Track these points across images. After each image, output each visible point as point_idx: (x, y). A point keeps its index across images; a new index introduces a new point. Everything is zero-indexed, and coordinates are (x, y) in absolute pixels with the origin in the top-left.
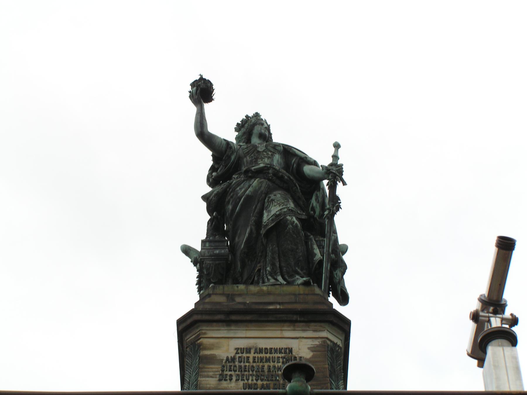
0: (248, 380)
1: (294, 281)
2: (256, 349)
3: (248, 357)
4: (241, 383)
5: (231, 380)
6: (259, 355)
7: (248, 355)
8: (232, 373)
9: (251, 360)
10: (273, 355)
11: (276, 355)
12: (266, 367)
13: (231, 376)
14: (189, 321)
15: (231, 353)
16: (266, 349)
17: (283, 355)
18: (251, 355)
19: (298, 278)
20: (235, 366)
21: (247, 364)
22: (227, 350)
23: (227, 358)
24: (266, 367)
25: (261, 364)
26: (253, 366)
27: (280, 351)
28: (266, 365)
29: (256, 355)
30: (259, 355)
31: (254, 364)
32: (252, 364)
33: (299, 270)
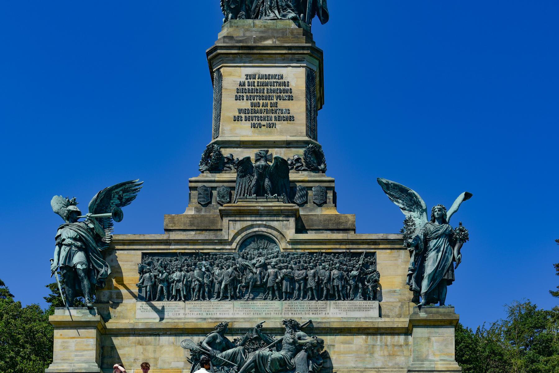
0: (254, 100)
1: (286, 15)
2: (259, 75)
3: (254, 82)
4: (249, 102)
5: (243, 99)
6: (261, 80)
7: (254, 80)
8: (244, 94)
9: (256, 84)
10: (270, 80)
11: (272, 80)
12: (266, 89)
13: (243, 96)
14: (214, 54)
15: (243, 79)
16: (266, 75)
17: (277, 80)
18: (256, 80)
19: (289, 12)
20: (245, 89)
21: (253, 87)
22: (240, 76)
23: (240, 82)
24: (266, 89)
25: (262, 87)
26: (257, 90)
27: (274, 76)
28: (265, 88)
29: (259, 80)
30: (261, 80)
31: (258, 88)
32: (256, 87)
33: (290, 4)
